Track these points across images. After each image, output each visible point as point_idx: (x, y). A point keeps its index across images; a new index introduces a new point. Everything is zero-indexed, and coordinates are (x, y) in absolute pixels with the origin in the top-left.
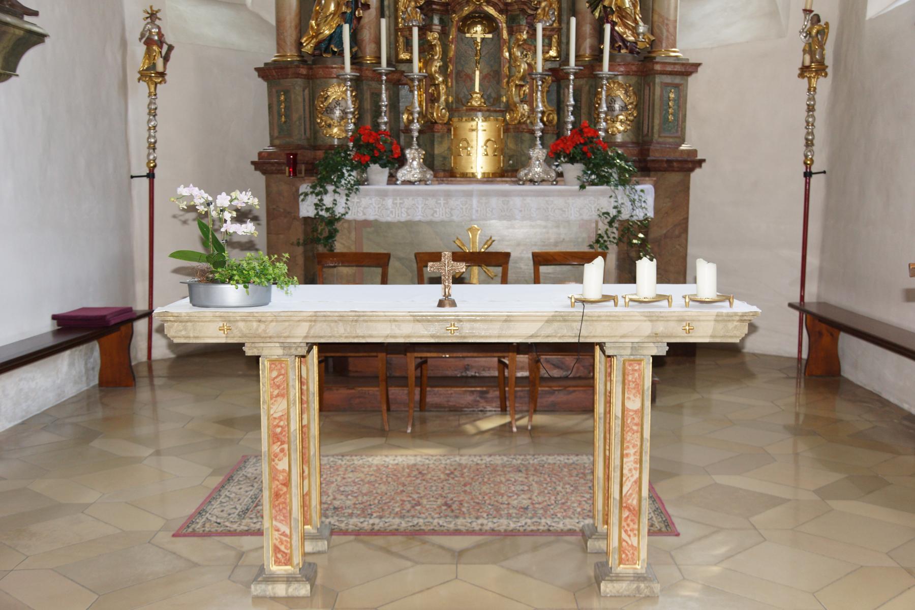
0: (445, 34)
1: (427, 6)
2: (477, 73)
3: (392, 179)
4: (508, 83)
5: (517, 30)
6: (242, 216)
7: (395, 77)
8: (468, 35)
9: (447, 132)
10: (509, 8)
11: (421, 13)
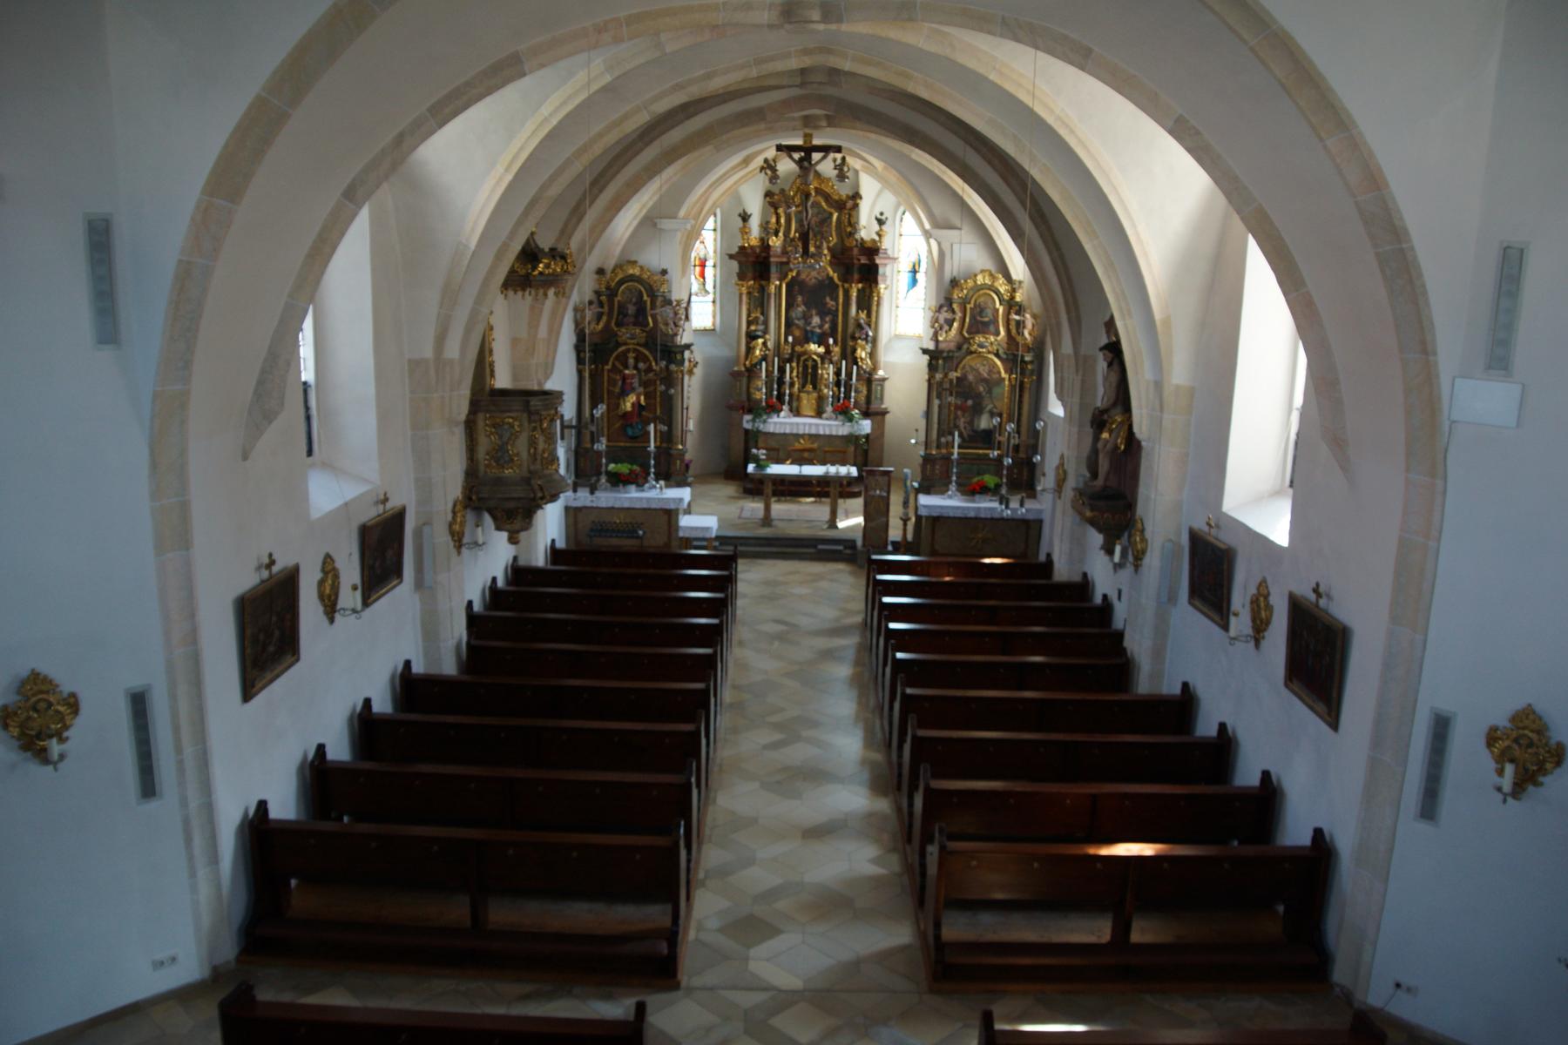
3: (778, 416)
6: (763, 454)
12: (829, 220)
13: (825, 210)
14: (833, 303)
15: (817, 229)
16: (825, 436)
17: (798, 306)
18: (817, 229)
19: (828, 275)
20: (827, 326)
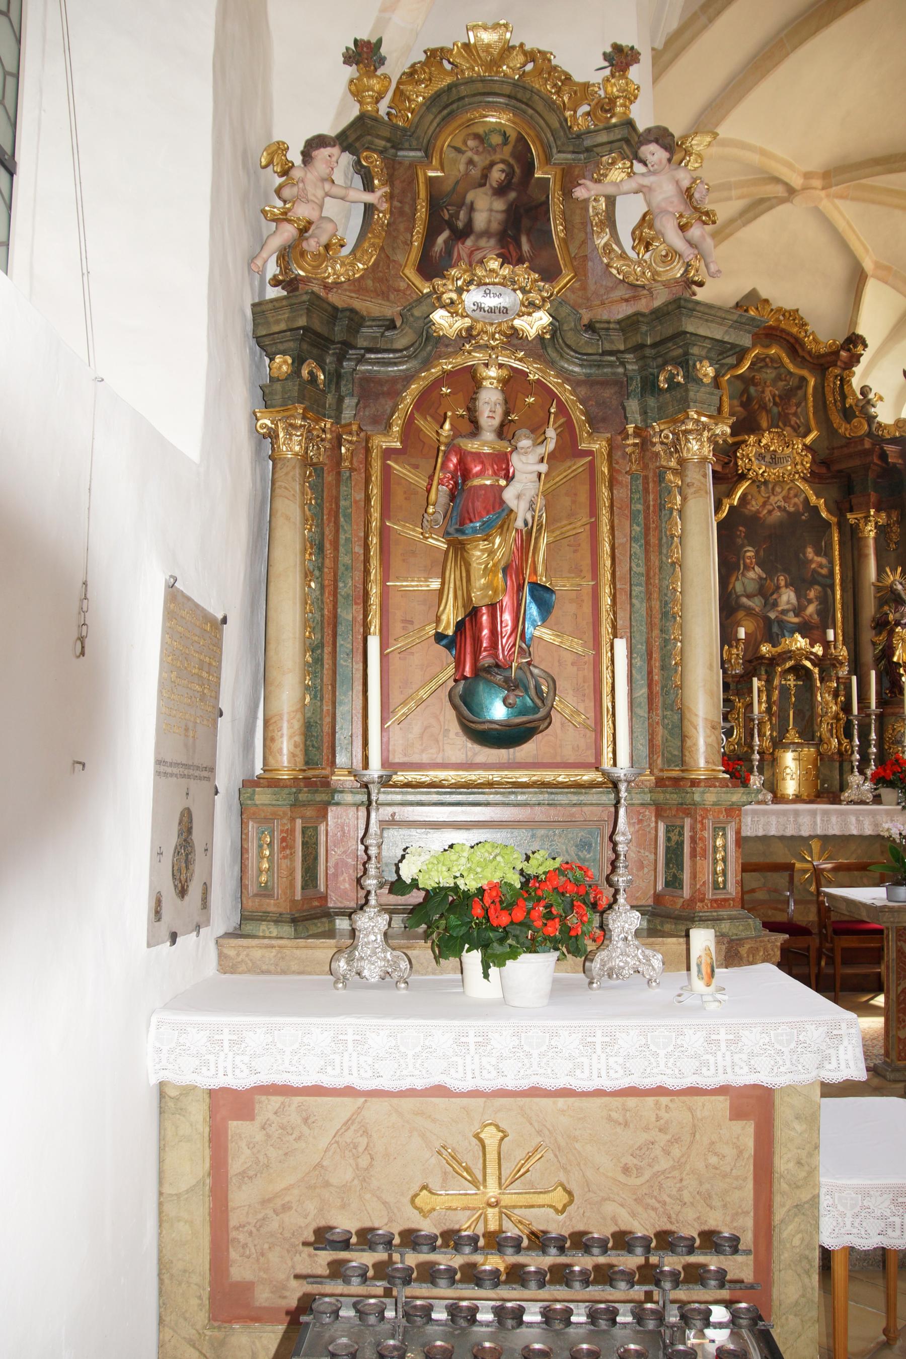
12: (800, 393)
13: (790, 373)
14: (823, 561)
15: (775, 410)
16: (862, 838)
17: (747, 568)
18: (775, 410)
19: (807, 500)
20: (811, 609)
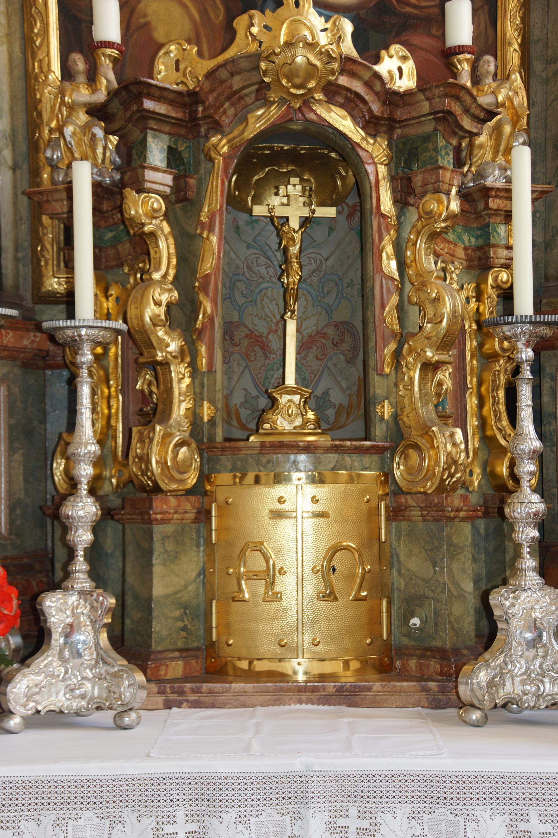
0: (185, 199)
1: (126, 105)
2: (291, 327)
4: (397, 355)
5: (425, 185)
7: (26, 342)
8: (259, 210)
9: (196, 520)
10: (399, 114)
11: (108, 132)
